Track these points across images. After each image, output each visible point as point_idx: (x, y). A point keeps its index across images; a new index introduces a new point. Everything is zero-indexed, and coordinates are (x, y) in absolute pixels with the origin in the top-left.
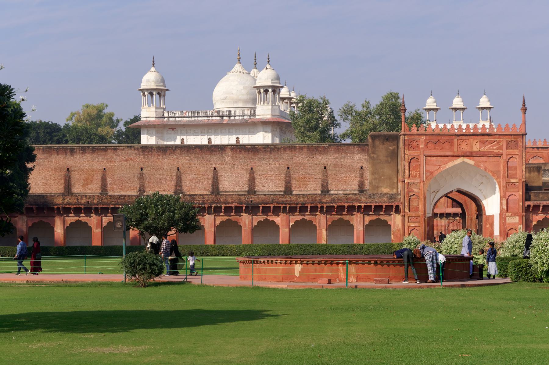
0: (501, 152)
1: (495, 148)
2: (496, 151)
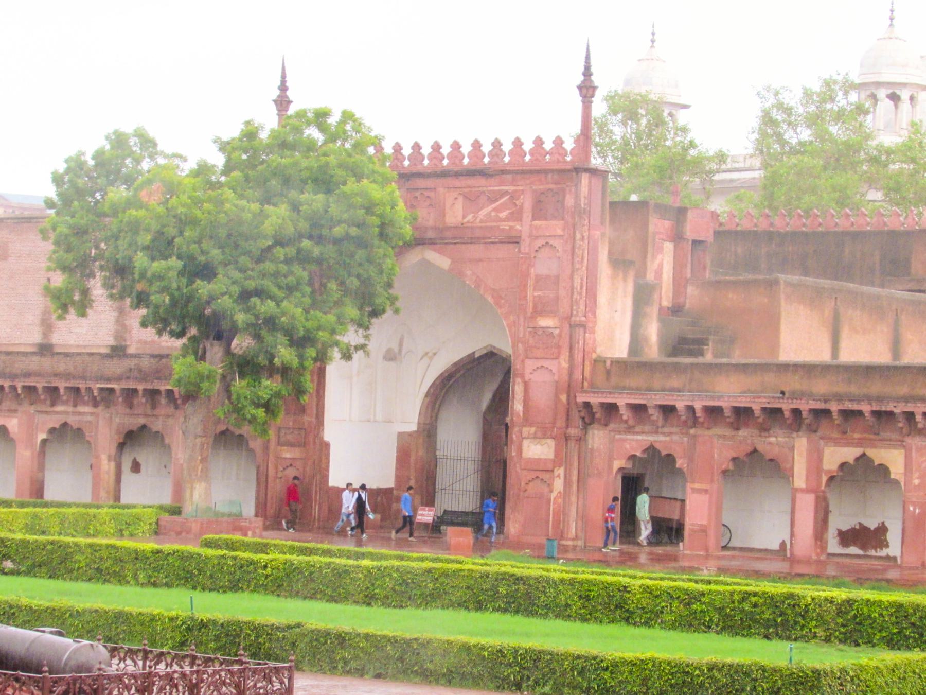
0: (518, 227)
1: (503, 215)
2: (505, 226)
